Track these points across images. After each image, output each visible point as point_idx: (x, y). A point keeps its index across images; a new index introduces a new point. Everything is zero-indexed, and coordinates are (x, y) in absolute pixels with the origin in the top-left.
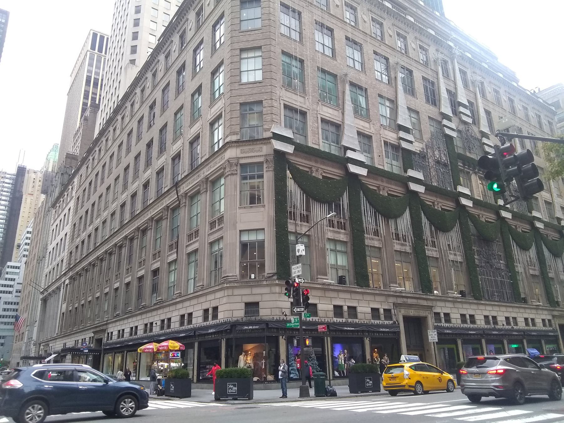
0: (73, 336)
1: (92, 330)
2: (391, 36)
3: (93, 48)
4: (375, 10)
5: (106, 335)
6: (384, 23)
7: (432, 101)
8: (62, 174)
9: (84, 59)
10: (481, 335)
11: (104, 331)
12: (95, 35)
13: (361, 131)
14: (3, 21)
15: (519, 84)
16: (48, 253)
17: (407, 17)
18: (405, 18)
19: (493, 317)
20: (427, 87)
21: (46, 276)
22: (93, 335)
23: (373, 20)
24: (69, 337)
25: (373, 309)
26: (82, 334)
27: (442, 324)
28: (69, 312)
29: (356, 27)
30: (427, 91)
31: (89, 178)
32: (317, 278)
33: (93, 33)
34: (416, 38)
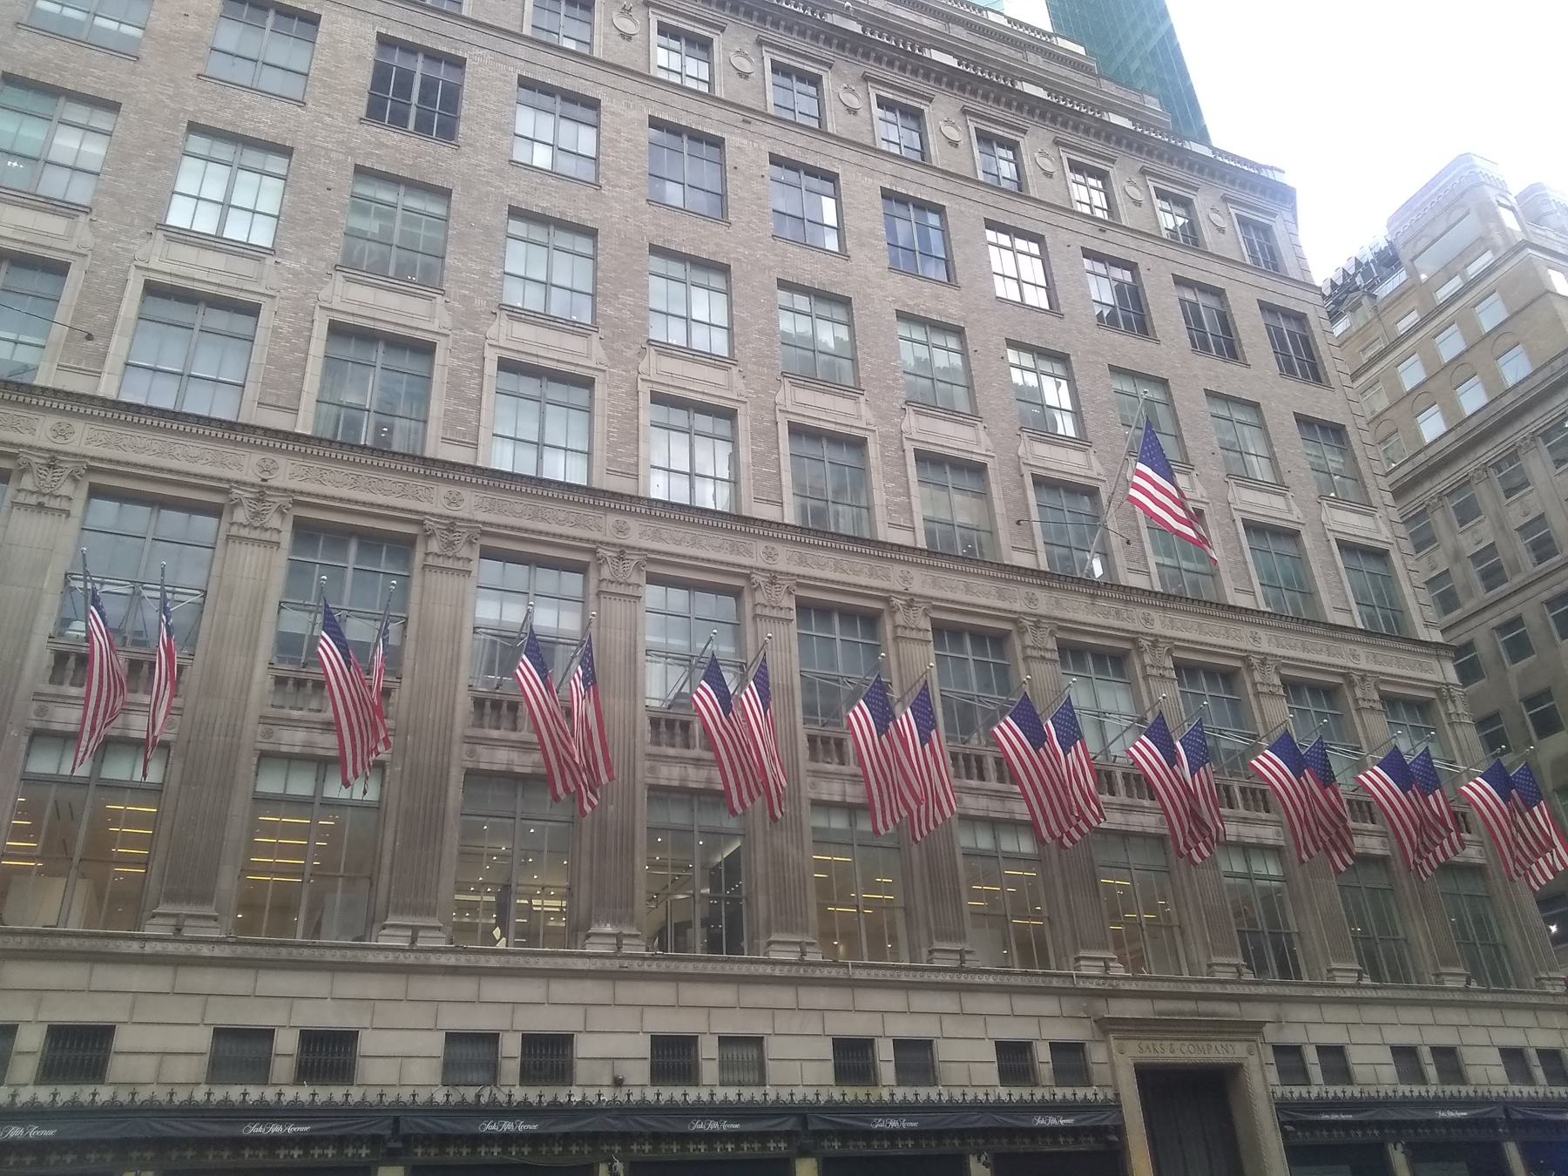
2: (1138, 203)
4: (977, 105)
6: (926, 110)
7: (1302, 368)
10: (375, 1141)
13: (664, 390)
15: (1215, 143)
17: (1018, 86)
18: (1012, 90)
19: (1322, 1050)
20: (1279, 331)
23: (883, 103)
25: (1003, 1048)
27: (1541, 1091)
29: (1113, 222)
30: (1283, 345)
32: (1078, 959)
34: (760, 43)
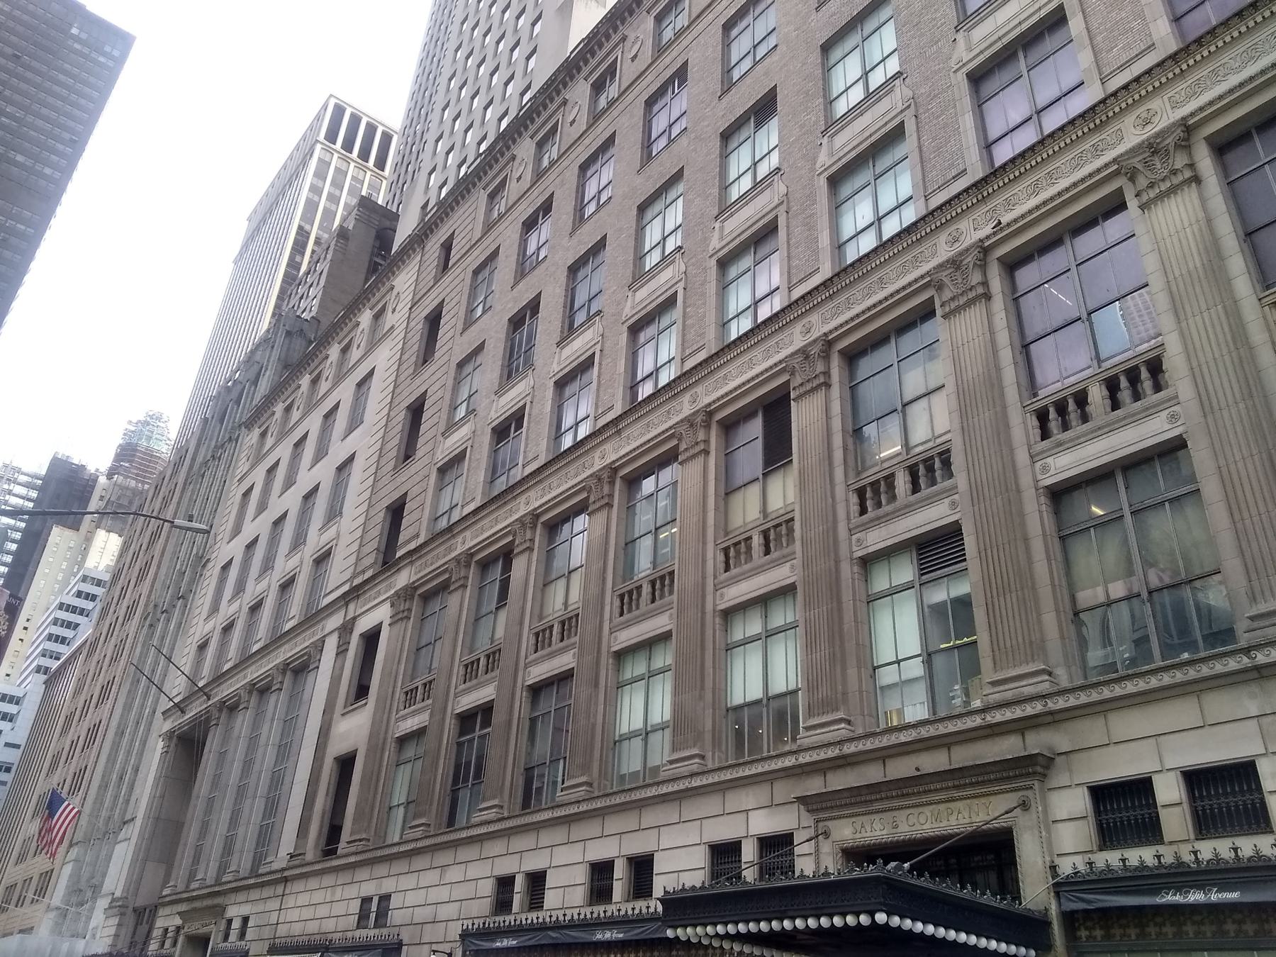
0: (465, 853)
1: (785, 790)
3: (332, 136)
5: (1071, 802)
8: (289, 333)
9: (304, 163)
11: (1030, 771)
12: (339, 111)
14: (116, 53)
16: (213, 571)
21: (203, 647)
22: (765, 823)
24: (420, 862)
26: (579, 831)
28: (391, 747)
31: (603, 124)
33: (336, 106)
